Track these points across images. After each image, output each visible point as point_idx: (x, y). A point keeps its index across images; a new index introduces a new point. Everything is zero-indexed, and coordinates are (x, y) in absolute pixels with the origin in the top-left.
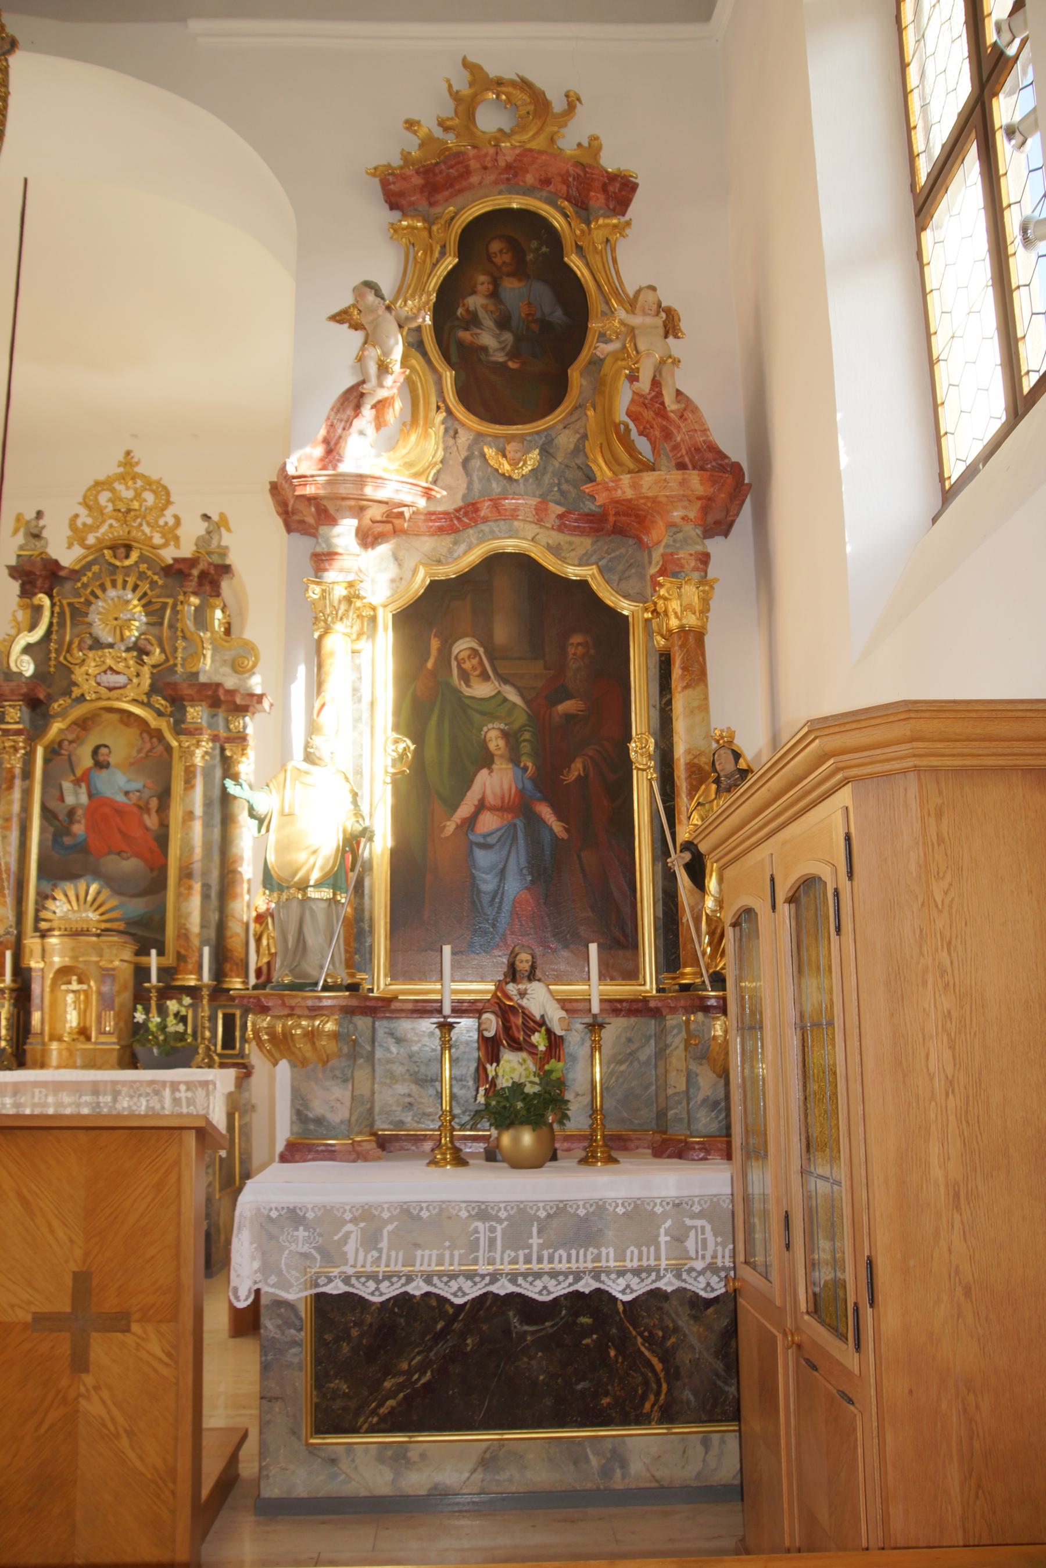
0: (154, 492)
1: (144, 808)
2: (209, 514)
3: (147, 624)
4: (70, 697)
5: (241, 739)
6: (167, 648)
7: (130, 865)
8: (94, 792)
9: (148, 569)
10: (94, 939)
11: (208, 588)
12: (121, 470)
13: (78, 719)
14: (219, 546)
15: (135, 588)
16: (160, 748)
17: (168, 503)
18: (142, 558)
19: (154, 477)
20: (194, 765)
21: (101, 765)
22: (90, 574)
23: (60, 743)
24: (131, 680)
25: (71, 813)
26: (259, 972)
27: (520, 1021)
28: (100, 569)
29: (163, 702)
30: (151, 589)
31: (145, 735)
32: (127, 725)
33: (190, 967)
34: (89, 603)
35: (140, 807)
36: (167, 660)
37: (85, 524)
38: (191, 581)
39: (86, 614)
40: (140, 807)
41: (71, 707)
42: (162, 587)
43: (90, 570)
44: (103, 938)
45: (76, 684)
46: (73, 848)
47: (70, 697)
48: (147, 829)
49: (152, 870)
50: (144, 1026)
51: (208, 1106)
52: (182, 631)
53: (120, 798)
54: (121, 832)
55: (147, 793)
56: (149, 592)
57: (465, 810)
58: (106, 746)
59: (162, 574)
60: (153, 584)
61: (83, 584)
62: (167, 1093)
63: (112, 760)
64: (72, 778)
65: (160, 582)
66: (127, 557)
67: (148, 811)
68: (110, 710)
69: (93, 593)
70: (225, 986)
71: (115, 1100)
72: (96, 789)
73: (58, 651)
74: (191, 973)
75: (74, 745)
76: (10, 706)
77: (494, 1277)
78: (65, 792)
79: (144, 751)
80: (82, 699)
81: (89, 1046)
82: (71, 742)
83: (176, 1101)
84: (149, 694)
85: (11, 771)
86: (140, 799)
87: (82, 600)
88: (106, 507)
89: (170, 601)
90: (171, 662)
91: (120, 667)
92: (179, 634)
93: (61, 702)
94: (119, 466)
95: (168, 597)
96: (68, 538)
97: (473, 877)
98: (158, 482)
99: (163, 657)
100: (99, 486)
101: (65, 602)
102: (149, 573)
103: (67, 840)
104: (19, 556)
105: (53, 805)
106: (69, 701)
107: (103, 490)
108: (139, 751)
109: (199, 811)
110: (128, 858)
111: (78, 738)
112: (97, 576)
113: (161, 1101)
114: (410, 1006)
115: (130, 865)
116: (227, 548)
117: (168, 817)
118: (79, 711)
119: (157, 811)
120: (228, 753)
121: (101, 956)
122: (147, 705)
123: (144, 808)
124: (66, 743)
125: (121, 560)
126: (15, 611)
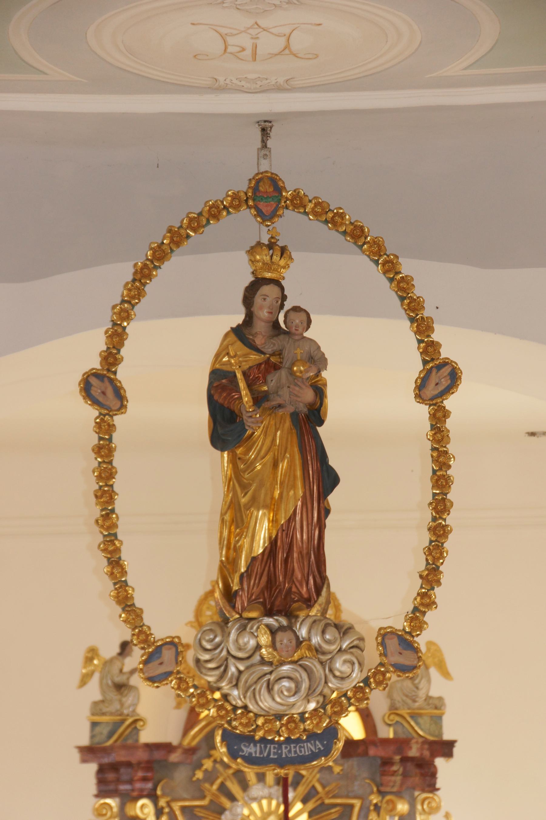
11: (417, 780)
14: (428, 698)
38: (394, 773)
56: (319, 788)
61: (206, 771)
65: (337, 769)
69: (224, 790)
89: (357, 803)
95: (356, 797)
101: (176, 806)
116: (440, 699)
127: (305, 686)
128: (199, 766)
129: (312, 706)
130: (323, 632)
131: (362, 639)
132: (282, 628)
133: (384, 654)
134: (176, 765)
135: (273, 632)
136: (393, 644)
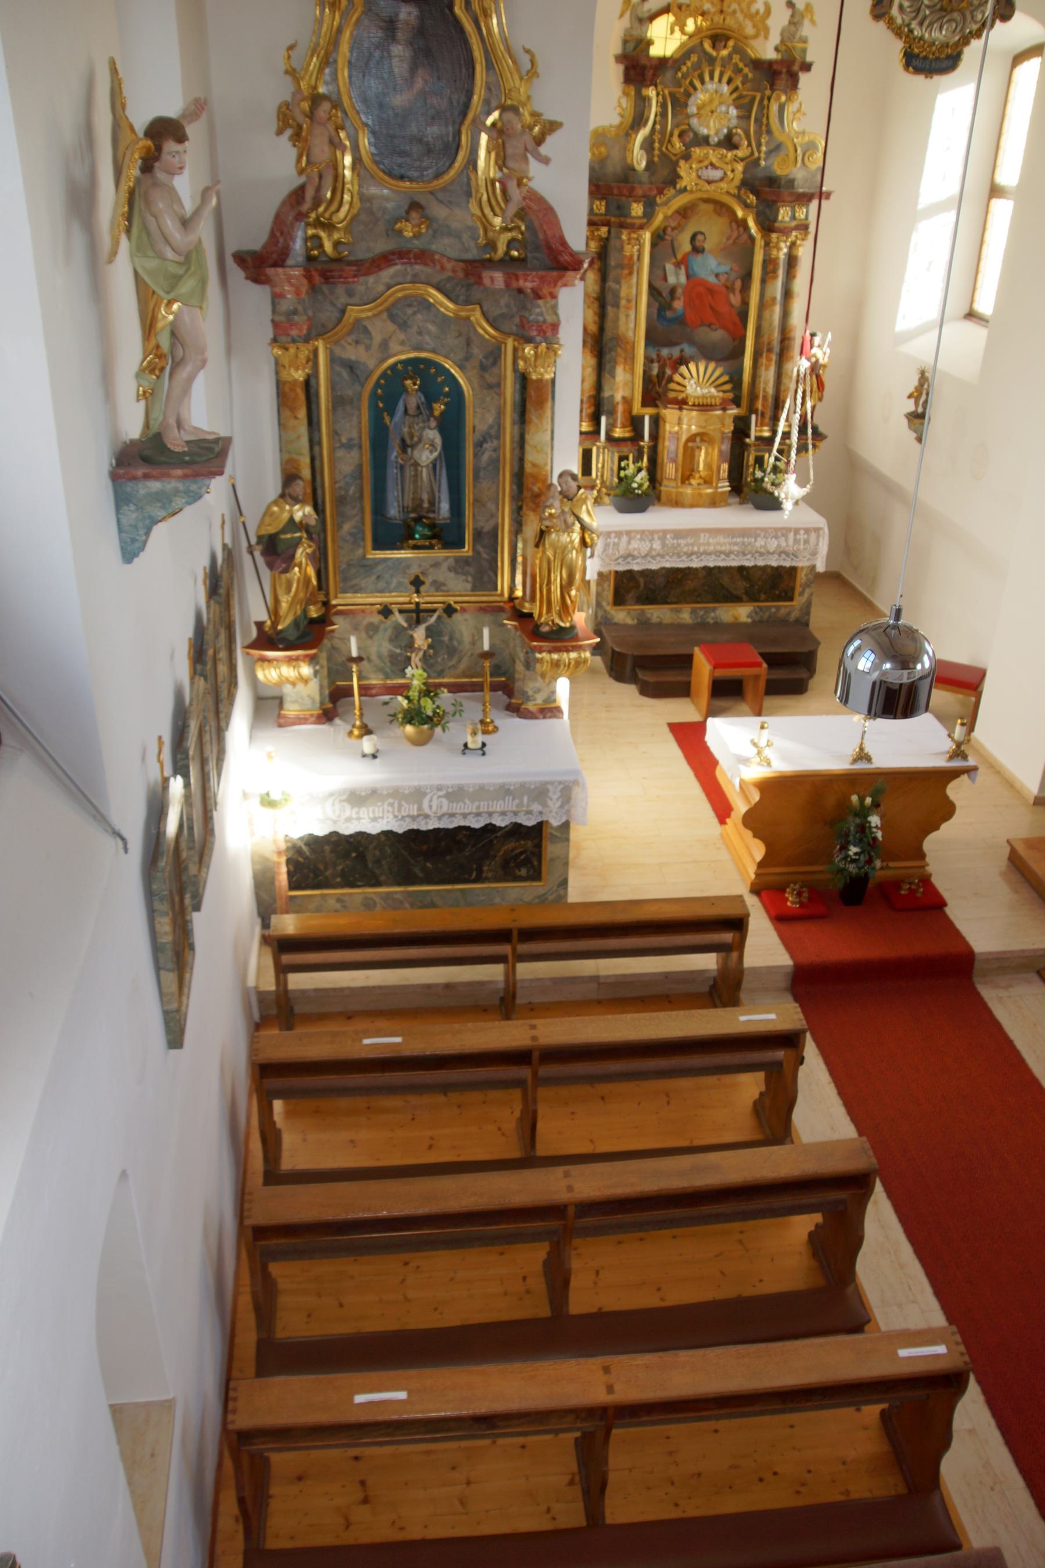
1: (730, 288)
4: (675, 188)
7: (718, 335)
8: (691, 272)
13: (680, 208)
16: (745, 237)
20: (777, 258)
21: (697, 250)
23: (665, 230)
24: (725, 174)
25: (673, 291)
29: (751, 196)
30: (743, 83)
31: (734, 225)
32: (719, 214)
34: (688, 95)
35: (727, 288)
36: (752, 153)
39: (686, 105)
40: (727, 288)
41: (674, 197)
45: (680, 177)
47: (675, 188)
48: (732, 306)
49: (734, 340)
51: (817, 544)
52: (768, 125)
53: (712, 279)
54: (711, 307)
55: (733, 275)
58: (702, 233)
62: (791, 535)
64: (674, 260)
67: (733, 290)
68: (706, 201)
69: (692, 84)
71: (756, 540)
72: (693, 269)
73: (661, 143)
74: (766, 426)
75: (676, 231)
76: (635, 202)
80: (685, 190)
82: (673, 229)
84: (739, 188)
85: (631, 256)
86: (727, 280)
87: (682, 90)
92: (764, 128)
103: (669, 314)
105: (658, 284)
108: (728, 239)
110: (716, 330)
111: (679, 225)
113: (786, 540)
115: (718, 335)
117: (748, 296)
119: (741, 291)
122: (738, 197)
123: (730, 288)
124: (669, 230)
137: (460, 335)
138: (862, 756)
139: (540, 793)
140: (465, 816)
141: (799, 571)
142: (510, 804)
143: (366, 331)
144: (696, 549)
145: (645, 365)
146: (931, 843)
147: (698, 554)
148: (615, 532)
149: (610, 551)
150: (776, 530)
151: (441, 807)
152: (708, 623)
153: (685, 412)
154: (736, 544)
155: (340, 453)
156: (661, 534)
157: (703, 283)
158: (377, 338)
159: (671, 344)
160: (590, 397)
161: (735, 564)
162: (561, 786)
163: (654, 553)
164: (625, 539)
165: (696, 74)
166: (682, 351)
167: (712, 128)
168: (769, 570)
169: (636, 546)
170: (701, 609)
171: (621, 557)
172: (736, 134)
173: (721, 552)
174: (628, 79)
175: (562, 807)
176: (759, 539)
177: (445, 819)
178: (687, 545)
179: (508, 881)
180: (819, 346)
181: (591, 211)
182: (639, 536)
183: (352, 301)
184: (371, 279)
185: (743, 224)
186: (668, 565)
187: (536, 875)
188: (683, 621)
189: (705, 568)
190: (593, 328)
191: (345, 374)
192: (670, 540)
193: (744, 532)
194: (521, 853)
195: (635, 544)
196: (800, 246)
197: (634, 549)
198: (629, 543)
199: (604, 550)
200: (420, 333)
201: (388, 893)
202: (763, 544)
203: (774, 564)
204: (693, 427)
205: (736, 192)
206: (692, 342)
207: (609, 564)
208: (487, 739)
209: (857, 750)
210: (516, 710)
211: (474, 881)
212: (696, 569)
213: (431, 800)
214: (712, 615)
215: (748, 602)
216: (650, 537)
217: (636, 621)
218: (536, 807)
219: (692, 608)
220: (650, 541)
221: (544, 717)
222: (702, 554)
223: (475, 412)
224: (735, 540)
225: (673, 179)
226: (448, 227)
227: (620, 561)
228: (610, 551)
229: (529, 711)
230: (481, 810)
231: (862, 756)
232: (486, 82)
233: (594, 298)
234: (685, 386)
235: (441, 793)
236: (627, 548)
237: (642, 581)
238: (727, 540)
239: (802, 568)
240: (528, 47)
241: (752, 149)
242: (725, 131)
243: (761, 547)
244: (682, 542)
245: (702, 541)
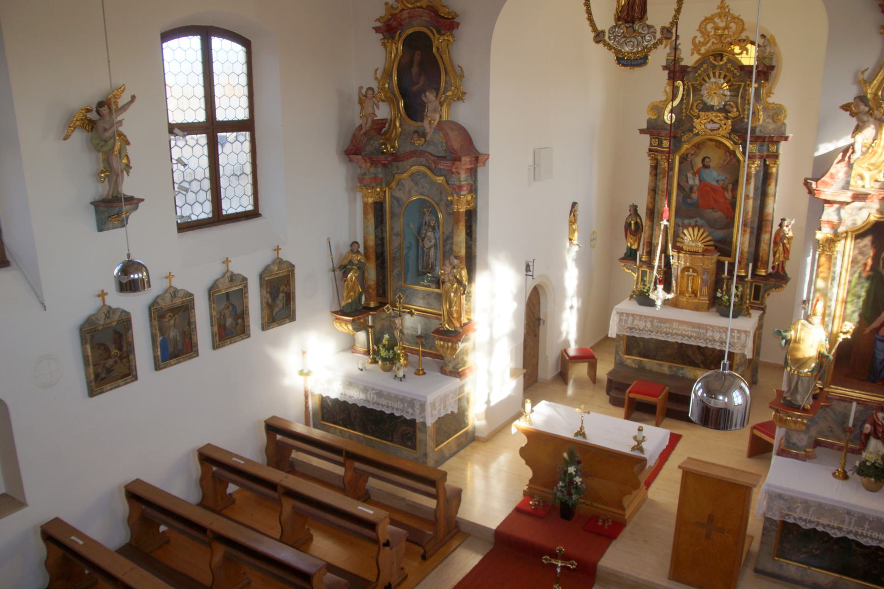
0: (736, 23)
2: (765, 35)
3: (730, 96)
5: (776, 156)
6: (740, 109)
7: (718, 215)
9: (732, 66)
10: (701, 256)
12: (719, 10)
15: (725, 77)
16: (734, 160)
17: (743, 29)
18: (729, 60)
19: (736, 14)
20: (751, 173)
22: (702, 69)
23: (687, 155)
24: (721, 126)
25: (691, 188)
26: (773, 268)
27: (881, 430)
28: (708, 66)
31: (727, 153)
32: (719, 148)
33: (742, 266)
34: (702, 85)
35: (723, 188)
36: (740, 115)
37: (700, 42)
39: (701, 90)
40: (723, 188)
41: (693, 138)
42: (738, 76)
43: (702, 67)
44: (705, 257)
45: (695, 127)
46: (691, 204)
48: (726, 199)
49: (727, 218)
50: (720, 298)
53: (714, 183)
56: (732, 79)
57: (876, 324)
58: (708, 158)
59: (739, 69)
60: (734, 75)
61: (699, 74)
63: (711, 164)
65: (738, 74)
66: (721, 60)
67: (727, 190)
68: (711, 140)
70: (757, 273)
71: (706, 332)
74: (742, 269)
77: (850, 532)
78: (689, 179)
79: (727, 161)
80: (697, 134)
81: (697, 301)
82: (692, 155)
83: (732, 337)
84: (730, 134)
88: (711, 32)
89: (743, 84)
90: (742, 116)
91: (716, 120)
92: (747, 102)
93: (688, 135)
94: (718, 9)
95: (742, 81)
96: (692, 49)
97: (874, 353)
98: (738, 18)
99: (738, 113)
100: (707, 20)
101: (690, 83)
102: (732, 69)
103: (689, 201)
104: (667, 60)
105: (683, 184)
106: (691, 135)
107: (709, 23)
108: (724, 161)
109: (751, 195)
111: (695, 152)
112: (706, 71)
113: (726, 335)
114: (837, 398)
115: (718, 215)
117: (736, 194)
118: (696, 140)
119: (731, 191)
120: (768, 163)
121: (704, 264)
122: (730, 139)
123: (725, 189)
124: (690, 155)
125: (718, 62)
126: (665, 87)
127: (636, 43)
128: (697, 72)
129: (640, 49)
130: (643, 28)
131: (656, 30)
132: (630, 26)
133: (662, 34)
134: (691, 72)
135: (627, 28)
136: (665, 31)
137: (438, 190)
138: (581, 433)
139: (411, 403)
140: (383, 406)
141: (735, 355)
142: (401, 406)
143: (403, 185)
144: (671, 331)
145: (674, 227)
146: (630, 503)
147: (672, 335)
148: (626, 313)
149: (623, 324)
150: (720, 328)
151: (374, 398)
152: (679, 376)
153: (681, 255)
154: (695, 332)
155: (394, 237)
156: (651, 319)
157: (709, 185)
158: (407, 189)
159: (691, 217)
160: (648, 242)
161: (693, 344)
162: (419, 403)
163: (646, 329)
164: (631, 318)
165: (705, 74)
166: (696, 222)
167: (715, 102)
168: (717, 352)
169: (637, 323)
170: (674, 366)
171: (628, 328)
172: (730, 105)
173: (686, 335)
174: (670, 78)
175: (420, 413)
176: (709, 332)
177: (375, 405)
178: (666, 328)
179: (402, 445)
180: (787, 226)
181: (651, 144)
182: (638, 318)
183: (399, 172)
184: (405, 163)
185: (733, 153)
186: (654, 337)
187: (414, 447)
188: (664, 372)
189: (677, 343)
190: (650, 206)
191: (396, 203)
192: (656, 323)
193: (699, 326)
194: (409, 433)
195: (636, 322)
196: (773, 167)
197: (636, 325)
198: (633, 320)
199: (619, 322)
200: (423, 188)
201: (358, 435)
202: (711, 334)
203: (718, 348)
204: (688, 264)
205: (728, 136)
206: (702, 218)
207: (622, 331)
208: (411, 375)
209: (579, 430)
210: (443, 371)
211: (391, 441)
212: (672, 343)
213: (370, 394)
214: (681, 372)
215: (704, 368)
216: (645, 320)
217: (637, 366)
218: (410, 411)
219: (669, 365)
220: (645, 322)
221: (451, 376)
222: (674, 334)
223: (443, 225)
224: (693, 329)
225: (691, 130)
226: (433, 142)
227: (628, 330)
228: (623, 324)
229: (446, 371)
230: (389, 405)
231: (581, 433)
232: (446, 80)
233: (652, 190)
234: (683, 239)
235: (374, 392)
236: (632, 324)
237: (641, 344)
238: (689, 329)
239: (737, 354)
240: (460, 65)
241: (739, 113)
242: (723, 103)
243: (710, 336)
244: (662, 325)
245: (674, 327)
